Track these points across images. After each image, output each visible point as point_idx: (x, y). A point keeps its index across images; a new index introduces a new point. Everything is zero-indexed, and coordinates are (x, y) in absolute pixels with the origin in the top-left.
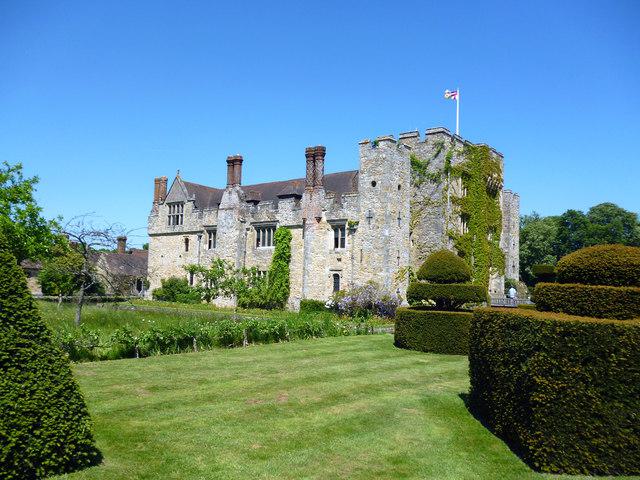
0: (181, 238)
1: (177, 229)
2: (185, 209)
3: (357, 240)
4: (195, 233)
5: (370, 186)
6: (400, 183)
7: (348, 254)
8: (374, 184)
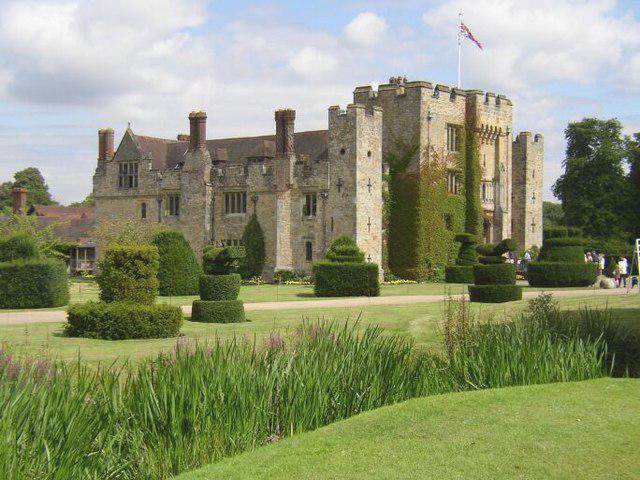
0: (135, 204)
1: (131, 192)
2: (139, 169)
3: (329, 208)
4: (154, 196)
5: (338, 152)
6: (370, 149)
7: (320, 222)
8: (343, 151)
